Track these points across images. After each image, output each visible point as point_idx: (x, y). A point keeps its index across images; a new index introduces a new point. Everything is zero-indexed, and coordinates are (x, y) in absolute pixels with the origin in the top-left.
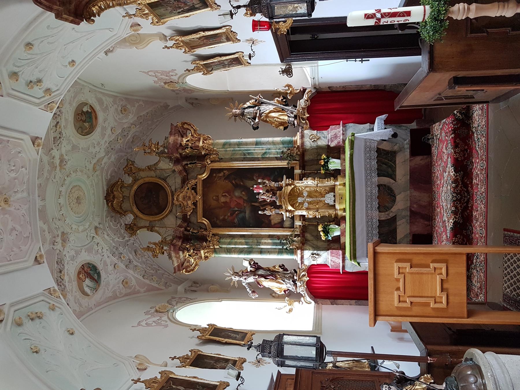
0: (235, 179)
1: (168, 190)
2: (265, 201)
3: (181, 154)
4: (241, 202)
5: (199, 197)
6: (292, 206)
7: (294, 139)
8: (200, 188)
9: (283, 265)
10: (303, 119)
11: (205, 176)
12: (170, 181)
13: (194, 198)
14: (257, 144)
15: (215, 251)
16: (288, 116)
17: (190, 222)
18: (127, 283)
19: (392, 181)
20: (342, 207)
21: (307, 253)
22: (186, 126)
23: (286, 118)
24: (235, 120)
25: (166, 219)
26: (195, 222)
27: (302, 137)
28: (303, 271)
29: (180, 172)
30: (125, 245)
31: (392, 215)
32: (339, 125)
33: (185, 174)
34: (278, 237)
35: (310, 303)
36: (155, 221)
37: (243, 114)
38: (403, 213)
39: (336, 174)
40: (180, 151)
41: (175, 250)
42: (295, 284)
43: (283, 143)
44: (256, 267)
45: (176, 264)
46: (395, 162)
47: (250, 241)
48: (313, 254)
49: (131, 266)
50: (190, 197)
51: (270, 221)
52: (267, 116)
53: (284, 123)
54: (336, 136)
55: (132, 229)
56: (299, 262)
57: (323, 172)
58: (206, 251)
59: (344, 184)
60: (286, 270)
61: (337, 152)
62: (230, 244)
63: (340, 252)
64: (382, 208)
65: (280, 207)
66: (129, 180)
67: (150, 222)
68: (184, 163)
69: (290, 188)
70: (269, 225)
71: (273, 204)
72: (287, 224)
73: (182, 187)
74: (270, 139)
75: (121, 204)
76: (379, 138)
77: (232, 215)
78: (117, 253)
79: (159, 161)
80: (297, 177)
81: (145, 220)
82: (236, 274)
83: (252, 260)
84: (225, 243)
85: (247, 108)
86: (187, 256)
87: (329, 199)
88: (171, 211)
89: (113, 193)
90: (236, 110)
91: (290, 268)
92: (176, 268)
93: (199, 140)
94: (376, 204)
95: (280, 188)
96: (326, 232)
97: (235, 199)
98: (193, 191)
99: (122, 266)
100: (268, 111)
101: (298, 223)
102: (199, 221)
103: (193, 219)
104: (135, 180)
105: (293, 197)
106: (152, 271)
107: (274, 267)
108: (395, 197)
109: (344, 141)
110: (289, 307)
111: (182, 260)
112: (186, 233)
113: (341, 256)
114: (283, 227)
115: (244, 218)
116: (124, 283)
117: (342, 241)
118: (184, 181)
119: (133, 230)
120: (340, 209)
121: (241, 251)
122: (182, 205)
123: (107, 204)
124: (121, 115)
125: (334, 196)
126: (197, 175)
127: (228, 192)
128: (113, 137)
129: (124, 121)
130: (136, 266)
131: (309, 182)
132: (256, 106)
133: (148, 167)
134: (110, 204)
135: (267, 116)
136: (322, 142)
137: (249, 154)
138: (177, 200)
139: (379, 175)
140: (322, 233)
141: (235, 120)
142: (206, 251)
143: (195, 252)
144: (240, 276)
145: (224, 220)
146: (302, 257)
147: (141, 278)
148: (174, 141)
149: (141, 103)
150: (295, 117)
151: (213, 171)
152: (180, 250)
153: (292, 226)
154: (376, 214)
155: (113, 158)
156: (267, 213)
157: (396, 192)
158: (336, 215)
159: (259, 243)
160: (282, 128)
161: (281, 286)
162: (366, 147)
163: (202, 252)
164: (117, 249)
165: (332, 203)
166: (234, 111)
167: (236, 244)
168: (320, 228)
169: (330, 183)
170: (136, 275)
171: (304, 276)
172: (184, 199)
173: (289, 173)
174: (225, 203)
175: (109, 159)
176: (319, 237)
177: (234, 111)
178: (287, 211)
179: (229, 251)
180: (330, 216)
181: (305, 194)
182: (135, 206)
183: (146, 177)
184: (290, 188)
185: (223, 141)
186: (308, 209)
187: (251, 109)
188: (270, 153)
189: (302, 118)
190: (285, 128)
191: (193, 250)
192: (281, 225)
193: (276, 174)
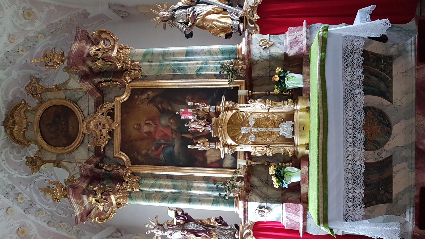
0: (162, 103)
1: (80, 116)
2: (196, 131)
3: (90, 68)
4: (168, 132)
5: (116, 125)
6: (233, 138)
7: (238, 47)
8: (117, 114)
9: (221, 218)
10: (252, 22)
11: (124, 97)
12: (83, 104)
13: (110, 126)
14: (188, 53)
15: (130, 196)
16: (232, 19)
17: (105, 157)
18: (23, 232)
19: (385, 102)
20: (304, 141)
21: (253, 206)
23: (229, 21)
24: (165, 27)
25: (76, 152)
26: (111, 157)
27: (249, 43)
28: (248, 228)
29: (91, 92)
30: (28, 183)
31: (385, 155)
32: (301, 25)
33: (99, 95)
34: (214, 180)
36: (63, 153)
38: (403, 153)
39: (297, 94)
40: (89, 63)
41: (74, 194)
43: (223, 52)
45: (78, 213)
46: (390, 73)
47: (179, 183)
48: (260, 207)
49: (33, 210)
50: (104, 125)
51: (205, 158)
53: (226, 28)
54: (296, 41)
55: (34, 163)
56: (242, 217)
57: (277, 91)
58: (118, 196)
59: (308, 110)
60: (226, 225)
61: (297, 63)
62: (153, 186)
63: (301, 207)
64: (370, 144)
65: (216, 140)
66: (33, 103)
67: (58, 155)
68: (97, 80)
69: (230, 114)
70: (204, 164)
71: (208, 136)
72: (228, 163)
73: (95, 112)
74: (206, 48)
75: (25, 132)
76: (366, 35)
77: (156, 149)
78: (11, 193)
79: (70, 79)
80: (242, 99)
81: (51, 153)
82: (160, 227)
83: (179, 209)
84: (146, 186)
86: (94, 202)
87: (285, 130)
88: (82, 142)
89: (13, 117)
90: (165, 13)
91: (231, 224)
92: (78, 217)
93: (113, 50)
94: (360, 137)
95: (217, 114)
96: (280, 177)
97: (160, 128)
98: (109, 117)
99: (19, 210)
100: (205, 13)
101: (242, 163)
102: (115, 156)
103: (109, 153)
104: (41, 102)
105: (235, 125)
106: (64, 216)
107: (209, 220)
108: (390, 126)
109: (308, 47)
111: (88, 207)
112: (97, 170)
113: (302, 213)
114: (222, 168)
115: (171, 154)
116: (19, 232)
117: (303, 189)
118: (98, 104)
119: (36, 165)
120: (301, 145)
121: (164, 198)
122: (94, 135)
123: (6, 131)
124: (24, 21)
125: (293, 126)
126: (115, 97)
127: (153, 119)
129: (29, 28)
130: (39, 210)
131: (258, 105)
133: (56, 86)
134: (8, 132)
136: (277, 50)
137: (180, 69)
138: (88, 128)
139: (366, 92)
140: (274, 179)
141: (165, 27)
142: (118, 196)
143: (104, 197)
144: (164, 230)
145: (147, 155)
146: (245, 211)
147: (45, 225)
148: (79, 49)
149: (52, 8)
150: (241, 20)
151: (134, 92)
152: (84, 192)
153: (234, 167)
154: (360, 155)
155: (15, 74)
156: (200, 147)
157: (392, 119)
158: (295, 154)
159: (190, 188)
162: (345, 50)
163: (112, 197)
164: (13, 188)
165: (290, 136)
167: (160, 186)
168: (272, 171)
169: (288, 107)
170: (39, 222)
172: (97, 126)
173: (232, 95)
174: (149, 133)
175: (8, 74)
176: (269, 184)
178: (225, 145)
179: (148, 197)
180: (286, 154)
181: (252, 122)
182: (39, 136)
183: (54, 98)
184: (230, 114)
185: (143, 50)
186: (254, 143)
187: (183, 10)
188: (207, 69)
189: (250, 20)
190: (228, 36)
191: (102, 194)
192: (219, 164)
193: (212, 95)
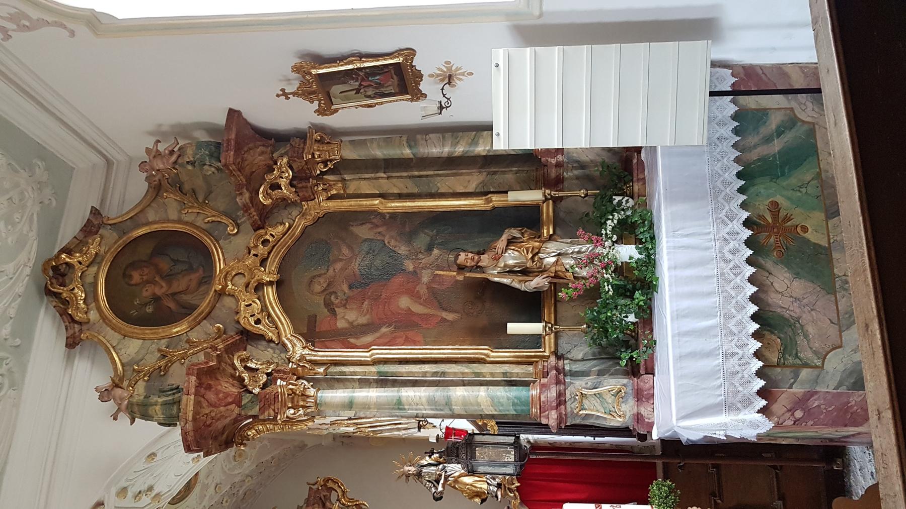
10: (511, 490)
22: (330, 484)
23: (485, 486)
24: (407, 481)
37: (419, 475)
52: (456, 481)
85: (426, 466)
90: (410, 468)
100: (457, 474)
124: (234, 463)
128: (217, 498)
132: (440, 463)
135: (456, 481)
141: (407, 481)
160: (478, 500)
166: (406, 468)
177: (406, 468)
187: (432, 468)
190: (483, 501)
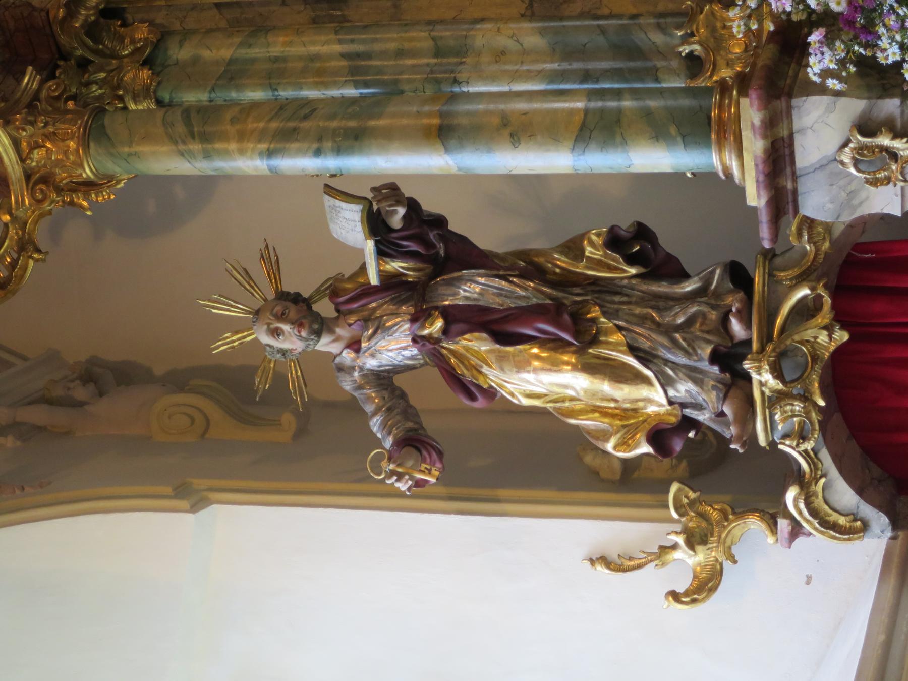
9: (642, 232)
28: (800, 280)
35: (855, 529)
42: (737, 383)
44: (423, 246)
48: (866, 127)
56: (755, 197)
82: (295, 307)
83: (391, 191)
110: (687, 562)
146: (779, 160)
161: (624, 393)
171: (805, 312)
